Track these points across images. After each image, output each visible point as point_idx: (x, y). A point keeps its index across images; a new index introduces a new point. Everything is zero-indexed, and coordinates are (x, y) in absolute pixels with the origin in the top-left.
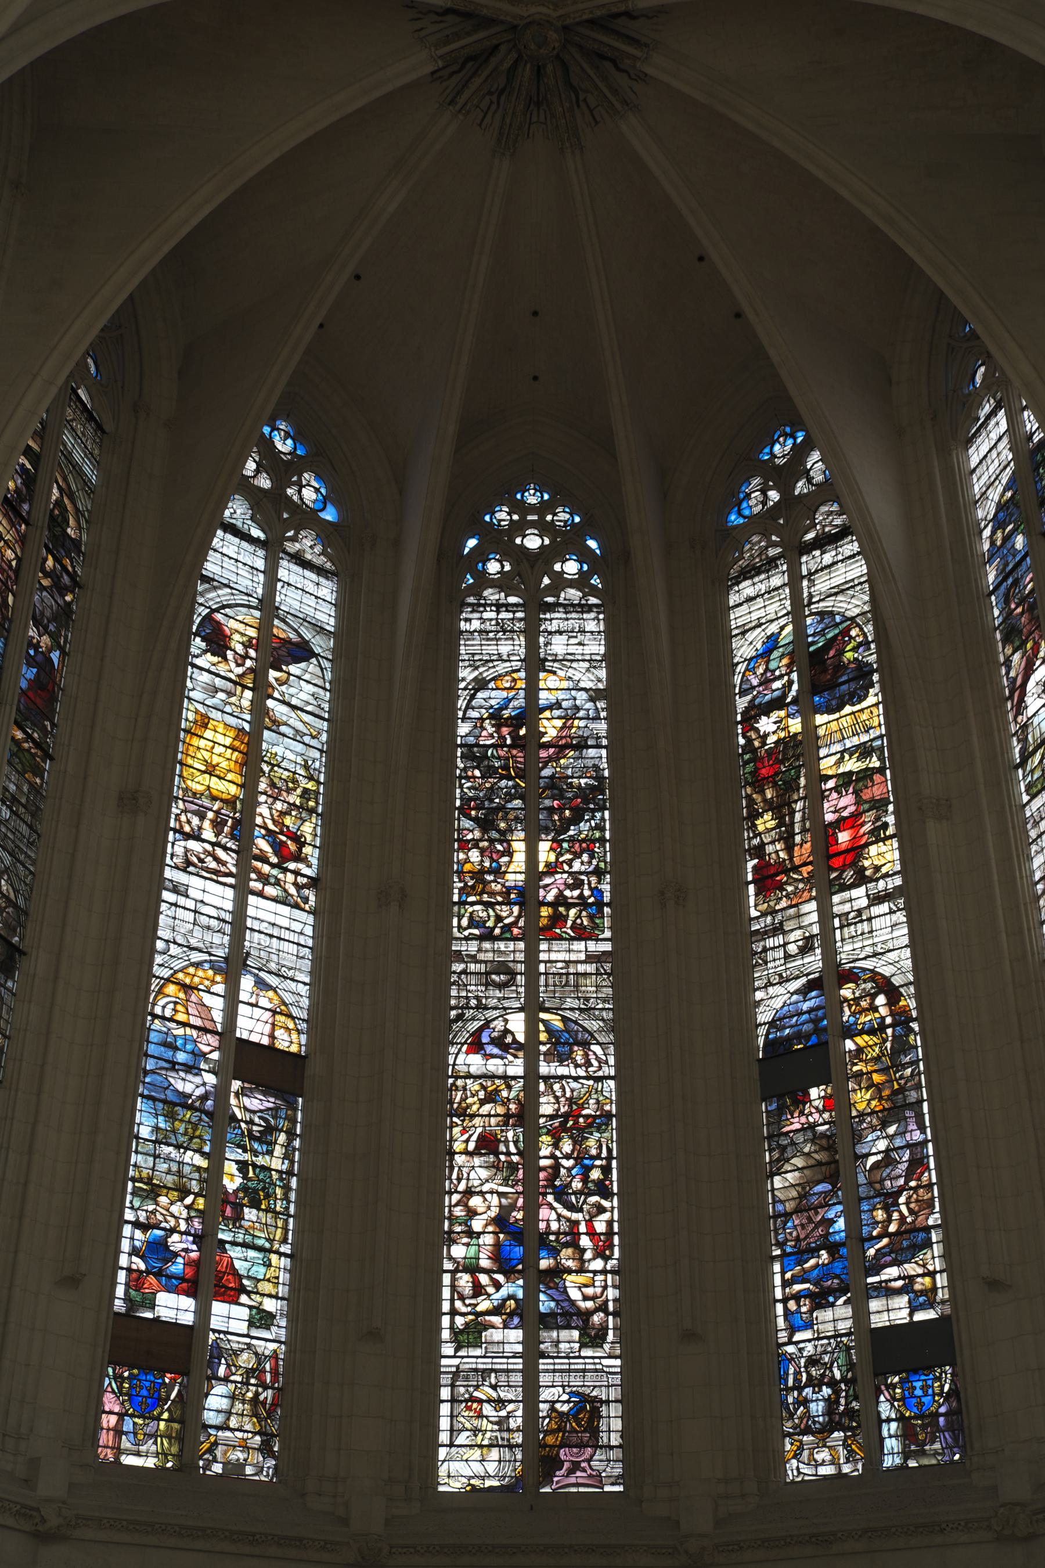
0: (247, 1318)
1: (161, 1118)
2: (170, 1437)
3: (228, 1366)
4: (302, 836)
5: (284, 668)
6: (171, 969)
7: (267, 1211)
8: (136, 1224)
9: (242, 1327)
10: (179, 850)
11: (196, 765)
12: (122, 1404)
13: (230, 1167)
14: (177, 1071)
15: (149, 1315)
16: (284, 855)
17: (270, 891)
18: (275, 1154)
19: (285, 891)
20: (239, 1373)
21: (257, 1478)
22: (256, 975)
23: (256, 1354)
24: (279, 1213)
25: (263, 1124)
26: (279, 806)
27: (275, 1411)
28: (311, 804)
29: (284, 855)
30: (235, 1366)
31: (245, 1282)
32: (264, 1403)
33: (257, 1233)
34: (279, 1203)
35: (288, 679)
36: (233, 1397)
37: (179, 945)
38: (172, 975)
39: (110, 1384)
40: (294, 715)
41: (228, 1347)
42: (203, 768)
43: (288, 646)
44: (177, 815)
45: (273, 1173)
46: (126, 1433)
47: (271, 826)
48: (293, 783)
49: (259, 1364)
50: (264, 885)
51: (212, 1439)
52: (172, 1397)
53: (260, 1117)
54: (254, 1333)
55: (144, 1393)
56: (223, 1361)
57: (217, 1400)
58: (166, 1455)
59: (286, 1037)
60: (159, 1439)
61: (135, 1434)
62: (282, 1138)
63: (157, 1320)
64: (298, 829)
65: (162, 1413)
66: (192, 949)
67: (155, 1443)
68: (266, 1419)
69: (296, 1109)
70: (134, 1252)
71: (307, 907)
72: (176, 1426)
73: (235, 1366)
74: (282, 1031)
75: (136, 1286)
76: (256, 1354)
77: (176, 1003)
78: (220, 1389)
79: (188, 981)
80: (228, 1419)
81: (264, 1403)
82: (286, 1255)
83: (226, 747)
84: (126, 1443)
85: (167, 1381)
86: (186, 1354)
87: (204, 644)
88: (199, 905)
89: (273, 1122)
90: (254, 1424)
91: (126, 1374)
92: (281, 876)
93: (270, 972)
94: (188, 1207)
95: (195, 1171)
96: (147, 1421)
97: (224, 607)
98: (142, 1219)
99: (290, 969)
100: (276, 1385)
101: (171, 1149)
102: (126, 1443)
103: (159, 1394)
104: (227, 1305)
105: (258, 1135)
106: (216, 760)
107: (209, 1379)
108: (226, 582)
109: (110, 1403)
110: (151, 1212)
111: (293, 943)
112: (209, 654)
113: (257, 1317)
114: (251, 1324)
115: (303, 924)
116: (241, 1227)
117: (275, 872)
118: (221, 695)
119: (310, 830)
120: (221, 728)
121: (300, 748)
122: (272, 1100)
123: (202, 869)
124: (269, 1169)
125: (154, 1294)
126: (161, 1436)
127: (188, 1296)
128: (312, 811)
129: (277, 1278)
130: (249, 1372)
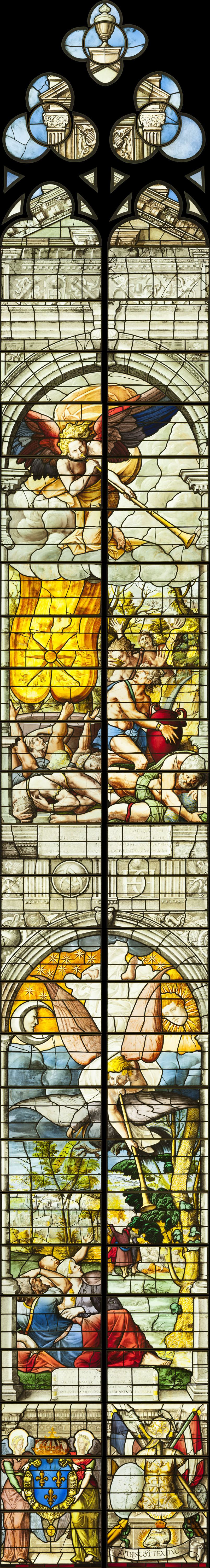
0: (155, 1382)
1: (35, 1161)
4: (180, 710)
5: (132, 451)
6: (27, 963)
7: (170, 1245)
8: (18, 1296)
9: (151, 1393)
10: (20, 796)
11: (31, 663)
12: (26, 1499)
13: (117, 1201)
14: (48, 1097)
16: (155, 748)
17: (140, 810)
18: (176, 1171)
19: (163, 803)
20: (151, 1445)
21: (182, 1561)
22: (130, 938)
24: (188, 1245)
25: (157, 1136)
26: (142, 677)
28: (192, 654)
29: (155, 748)
30: (145, 1438)
31: (150, 1338)
32: (186, 1476)
33: (160, 1276)
34: (186, 1231)
35: (139, 466)
37: (34, 929)
38: (28, 974)
40: (154, 523)
42: (39, 663)
43: (136, 410)
44: (12, 746)
45: (174, 1195)
47: (133, 714)
48: (160, 632)
50: (130, 804)
51: (123, 1524)
52: (83, 1486)
53: (152, 1129)
59: (179, 1011)
61: (45, 1530)
62: (185, 1147)
64: (174, 701)
66: (49, 928)
67: (70, 1537)
69: (200, 1105)
70: (20, 1328)
71: (194, 817)
73: (145, 1438)
74: (173, 1004)
77: (37, 1008)
78: (128, 1468)
79: (49, 975)
81: (186, 1476)
82: (201, 1296)
83: (70, 616)
87: (22, 466)
88: (54, 864)
89: (169, 1131)
90: (174, 1501)
91: (26, 1467)
92: (154, 784)
93: (149, 928)
94: (79, 1263)
95: (84, 1217)
97: (44, 391)
98: (24, 1290)
99: (176, 914)
101: (51, 1196)
105: (152, 1151)
106: (57, 641)
108: (42, 345)
109: (11, 1501)
110: (35, 1278)
111: (180, 875)
112: (31, 479)
113: (170, 1378)
114: (161, 1387)
115: (192, 841)
116: (139, 1272)
117: (143, 781)
118: (55, 538)
119: (190, 697)
120: (59, 589)
121: (166, 573)
122: (167, 1101)
123: (55, 812)
124: (169, 1192)
128: (191, 667)
129: (192, 1326)
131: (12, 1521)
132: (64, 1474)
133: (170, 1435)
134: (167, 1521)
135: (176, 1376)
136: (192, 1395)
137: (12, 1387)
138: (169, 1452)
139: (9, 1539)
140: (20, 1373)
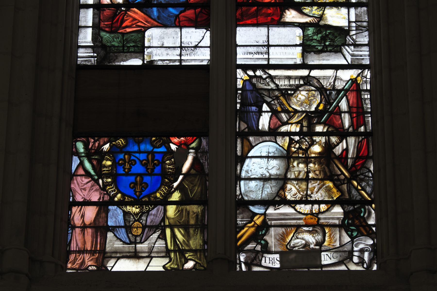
2: (185, 227)
3: (274, 113)
15: (137, 62)
23: (321, 89)
27: (364, 166)
36: (287, 157)
39: (81, 164)
41: (272, 86)
46: (113, 229)
49: (328, 103)
54: (313, 60)
55: (138, 169)
56: (265, 107)
57: (260, 163)
58: (182, 252)
60: (168, 232)
63: (150, 66)
65: (170, 194)
68: (349, 181)
72: (195, 209)
75: (111, 26)
76: (321, 89)
80: (283, 188)
84: (113, 243)
85: (173, 147)
86: (212, 108)
90: (328, 190)
96: (145, 208)
100: (362, 129)
102: (113, 243)
103: (164, 169)
104: (263, 30)
107: (244, 136)
109: (83, 189)
113: (318, 37)
114: (307, 48)
125: (142, 33)
126: (172, 227)
127: (197, 26)
130: (311, 118)
131: (83, 216)
132: (158, 157)
133: (321, 107)
134: (321, 216)
135: (327, 36)
136: (349, 58)
137: (90, 50)
138: (319, 129)
139: (77, 240)
140: (103, 34)
